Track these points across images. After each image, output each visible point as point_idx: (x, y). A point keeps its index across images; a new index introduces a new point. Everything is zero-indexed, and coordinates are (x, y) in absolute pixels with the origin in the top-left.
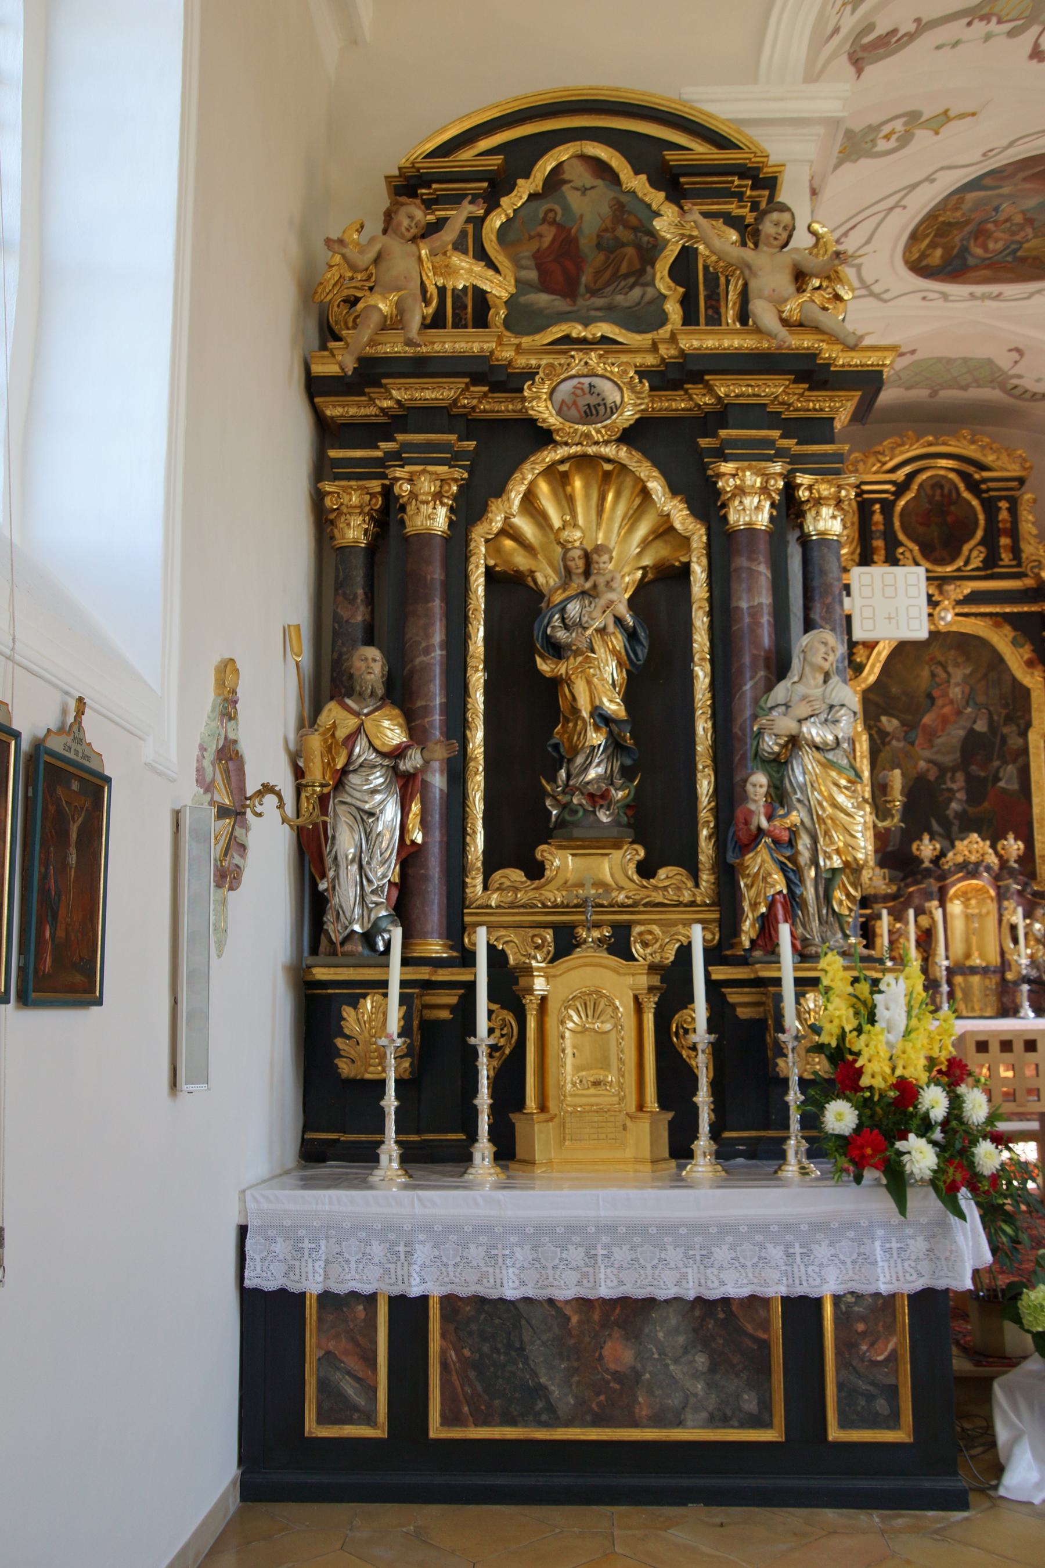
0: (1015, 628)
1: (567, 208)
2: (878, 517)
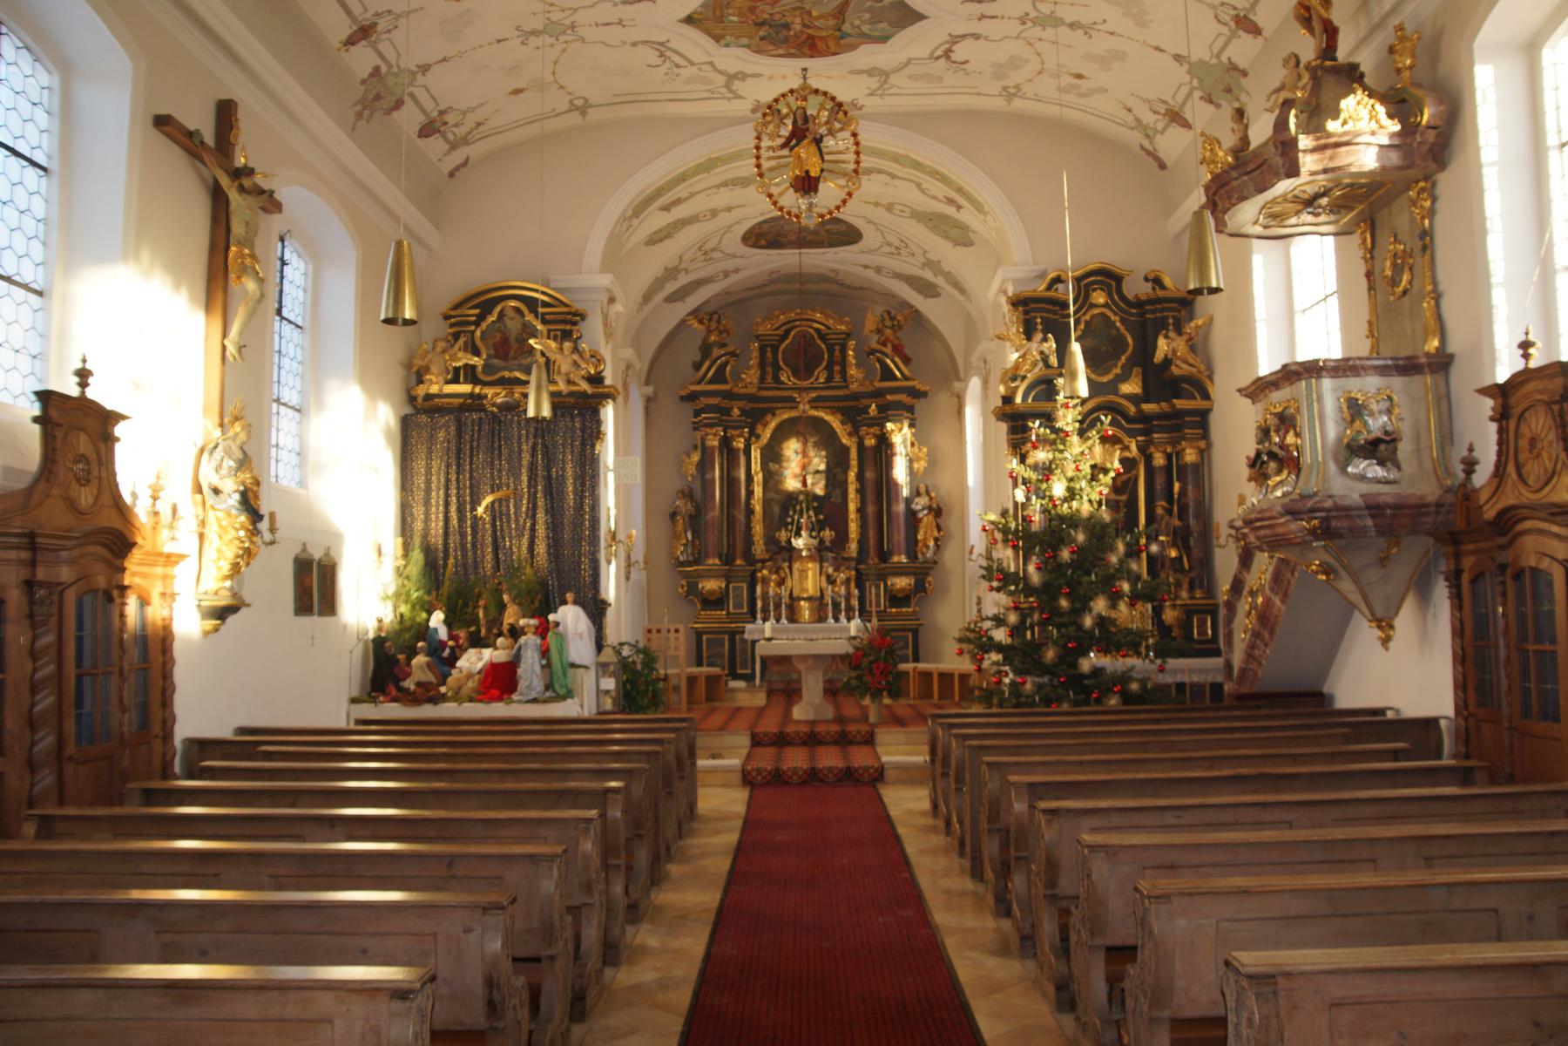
0: (843, 415)
1: (505, 326)
2: (769, 355)
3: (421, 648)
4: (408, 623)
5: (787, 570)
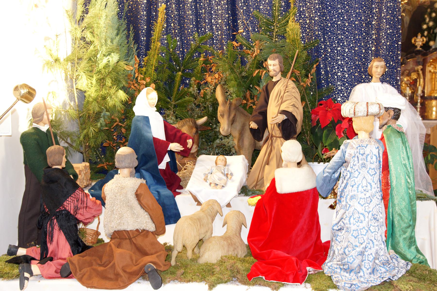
3: (125, 156)
4: (94, 107)
5: (421, 72)
